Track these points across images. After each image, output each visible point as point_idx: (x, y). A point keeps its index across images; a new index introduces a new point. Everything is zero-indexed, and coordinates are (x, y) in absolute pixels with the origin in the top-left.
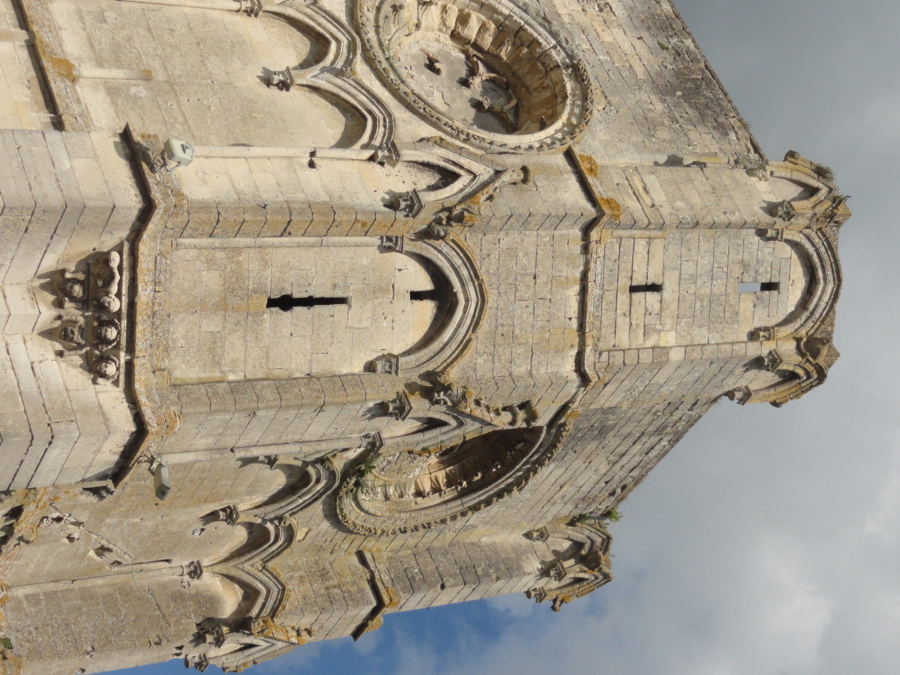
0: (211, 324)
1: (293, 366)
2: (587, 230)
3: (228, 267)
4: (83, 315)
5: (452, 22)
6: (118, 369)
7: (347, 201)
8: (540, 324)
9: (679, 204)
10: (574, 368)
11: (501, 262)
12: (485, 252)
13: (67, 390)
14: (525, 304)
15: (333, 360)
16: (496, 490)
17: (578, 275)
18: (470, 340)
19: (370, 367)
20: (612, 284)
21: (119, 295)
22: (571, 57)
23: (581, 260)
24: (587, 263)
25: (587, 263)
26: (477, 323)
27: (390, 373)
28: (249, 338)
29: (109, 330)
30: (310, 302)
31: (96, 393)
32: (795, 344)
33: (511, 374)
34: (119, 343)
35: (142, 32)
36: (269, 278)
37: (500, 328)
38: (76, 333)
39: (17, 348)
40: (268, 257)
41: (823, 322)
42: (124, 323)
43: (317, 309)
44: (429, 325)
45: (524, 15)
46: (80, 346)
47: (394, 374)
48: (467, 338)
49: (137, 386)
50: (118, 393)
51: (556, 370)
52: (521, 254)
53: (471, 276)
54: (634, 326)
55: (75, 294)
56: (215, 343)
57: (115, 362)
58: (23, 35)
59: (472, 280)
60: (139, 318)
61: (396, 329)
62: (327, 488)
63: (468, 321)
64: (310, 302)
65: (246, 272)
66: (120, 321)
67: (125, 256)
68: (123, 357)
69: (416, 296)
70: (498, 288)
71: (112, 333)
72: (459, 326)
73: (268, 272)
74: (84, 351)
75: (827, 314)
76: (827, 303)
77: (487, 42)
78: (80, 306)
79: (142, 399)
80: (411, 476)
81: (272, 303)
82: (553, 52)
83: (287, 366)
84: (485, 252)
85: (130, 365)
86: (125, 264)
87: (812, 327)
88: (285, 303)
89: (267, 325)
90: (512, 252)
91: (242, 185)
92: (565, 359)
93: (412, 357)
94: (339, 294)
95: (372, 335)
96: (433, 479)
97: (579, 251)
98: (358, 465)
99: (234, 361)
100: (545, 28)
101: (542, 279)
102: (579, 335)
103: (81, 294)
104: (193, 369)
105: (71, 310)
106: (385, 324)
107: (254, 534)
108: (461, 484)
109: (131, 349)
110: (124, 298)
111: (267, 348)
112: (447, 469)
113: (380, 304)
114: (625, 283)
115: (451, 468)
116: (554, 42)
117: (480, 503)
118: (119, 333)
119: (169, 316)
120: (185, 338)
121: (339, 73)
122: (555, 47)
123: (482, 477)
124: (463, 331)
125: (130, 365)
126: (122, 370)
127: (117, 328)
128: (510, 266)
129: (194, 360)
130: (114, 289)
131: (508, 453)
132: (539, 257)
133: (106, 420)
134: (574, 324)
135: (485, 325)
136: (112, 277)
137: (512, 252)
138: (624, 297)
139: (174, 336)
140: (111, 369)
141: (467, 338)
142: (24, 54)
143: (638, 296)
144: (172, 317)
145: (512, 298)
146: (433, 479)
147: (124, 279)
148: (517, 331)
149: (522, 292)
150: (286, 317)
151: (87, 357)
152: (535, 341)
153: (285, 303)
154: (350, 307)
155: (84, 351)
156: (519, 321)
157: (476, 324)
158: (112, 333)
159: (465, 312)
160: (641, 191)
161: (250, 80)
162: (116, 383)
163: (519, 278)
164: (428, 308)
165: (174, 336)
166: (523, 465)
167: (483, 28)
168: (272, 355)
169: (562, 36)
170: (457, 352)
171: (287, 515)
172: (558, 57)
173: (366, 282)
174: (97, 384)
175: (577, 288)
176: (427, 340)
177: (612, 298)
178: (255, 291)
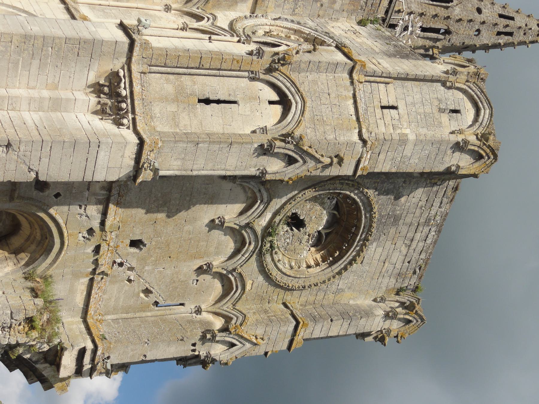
0: (172, 108)
1: (215, 130)
2: (351, 73)
3: (177, 83)
4: (110, 101)
6: (129, 121)
8: (336, 116)
10: (358, 138)
11: (310, 86)
12: (301, 81)
13: (105, 129)
14: (326, 106)
15: (234, 129)
16: (348, 260)
17: (351, 95)
18: (301, 120)
20: (370, 104)
21: (125, 88)
23: (351, 88)
24: (354, 90)
25: (354, 90)
26: (303, 113)
27: (264, 133)
28: (191, 115)
29: (122, 104)
30: (218, 102)
31: (119, 131)
32: (475, 137)
33: (325, 138)
34: (128, 110)
36: (197, 89)
37: (316, 117)
38: (108, 109)
40: (195, 80)
41: (488, 127)
42: (129, 101)
43: (223, 105)
44: (280, 116)
45: (316, 33)
46: (111, 115)
47: (265, 134)
48: (299, 119)
49: (138, 128)
50: (131, 131)
51: (349, 138)
52: (319, 83)
53: (296, 91)
54: (387, 125)
55: (105, 91)
56: (174, 116)
57: (127, 118)
59: (297, 93)
60: (135, 98)
61: (264, 116)
62: (256, 248)
63: (299, 112)
64: (218, 102)
65: (185, 86)
66: (127, 100)
67: (126, 71)
69: (271, 103)
70: (311, 98)
71: (124, 105)
72: (295, 114)
73: (196, 87)
74: (112, 117)
75: (489, 124)
76: (488, 119)
78: (108, 97)
80: (302, 257)
81: (200, 101)
83: (212, 129)
84: (301, 81)
85: (134, 120)
86: (126, 74)
87: (483, 130)
88: (207, 101)
89: (199, 110)
90: (315, 82)
92: (353, 134)
94: (232, 99)
95: (252, 119)
96: (315, 259)
97: (349, 84)
98: (268, 229)
99: (185, 125)
100: (327, 36)
101: (333, 95)
102: (357, 123)
103: (108, 91)
104: (166, 128)
105: (104, 99)
106: (258, 114)
107: (225, 287)
108: (329, 259)
109: (133, 112)
110: (127, 89)
111: (201, 121)
112: (321, 253)
113: (254, 104)
114: (377, 104)
115: (323, 252)
116: (332, 40)
117: (341, 270)
118: (127, 105)
119: (151, 103)
120: (160, 113)
122: (333, 42)
123: (339, 254)
124: (297, 116)
125: (134, 120)
126: (131, 122)
127: (126, 103)
128: (315, 89)
129: (166, 124)
130: (122, 85)
131: (349, 236)
132: (329, 85)
134: (354, 118)
135: (307, 114)
136: (121, 80)
137: (315, 82)
139: (155, 112)
140: (125, 121)
141: (299, 119)
143: (386, 111)
144: (152, 104)
145: (319, 103)
146: (315, 259)
147: (126, 81)
148: (325, 119)
152: (335, 124)
153: (207, 101)
154: (239, 105)
155: (112, 117)
156: (325, 114)
157: (303, 113)
158: (124, 105)
159: (296, 108)
162: (128, 128)
163: (321, 94)
165: (155, 112)
166: (358, 242)
168: (203, 124)
170: (296, 126)
171: (238, 267)
173: (245, 94)
174: (120, 128)
175: (352, 101)
177: (372, 110)
178: (191, 95)
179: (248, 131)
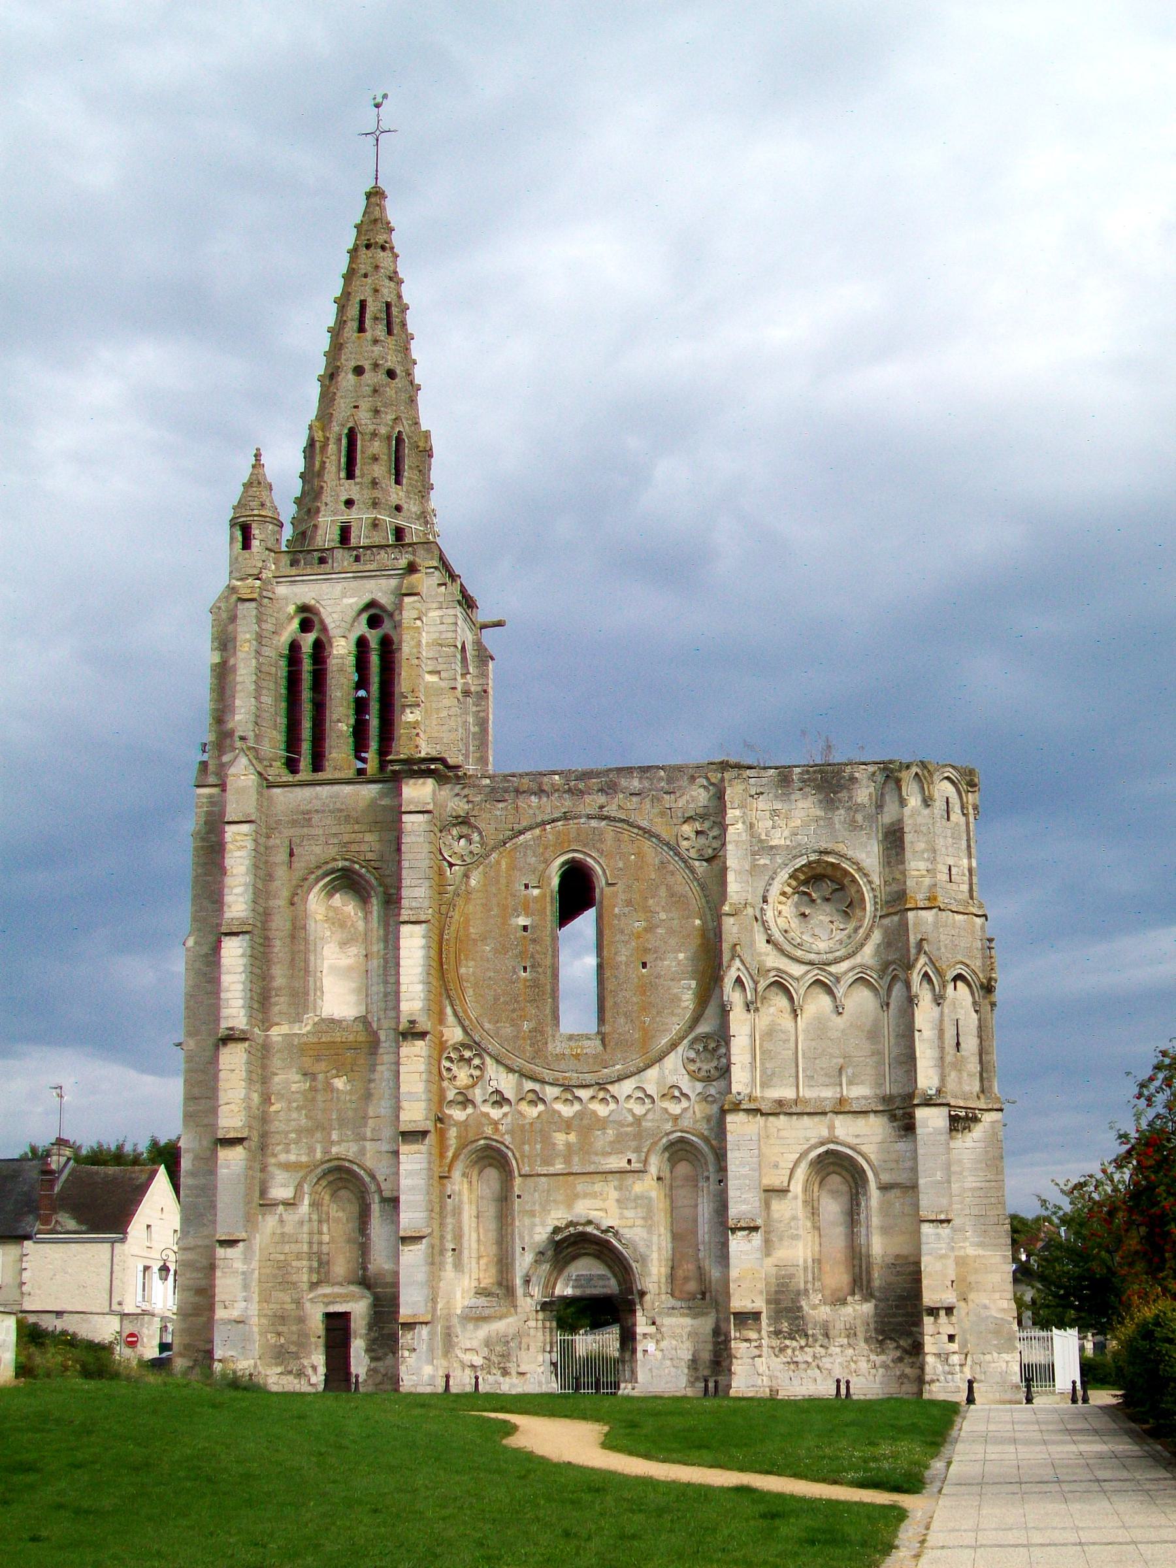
0: (965, 1075)
2: (940, 910)
5: (784, 899)
7: (938, 1022)
9: (926, 855)
19: (976, 1011)
22: (815, 852)
30: (958, 1034)
35: (817, 1061)
39: (967, 1145)
58: (830, 1115)
64: (958, 1034)
68: (977, 1112)
71: (970, 1115)
77: (794, 883)
79: (990, 1106)
82: (811, 859)
85: (980, 1110)
88: (958, 1044)
91: (932, 1063)
93: (976, 995)
109: (974, 1109)
114: (949, 886)
121: (838, 980)
125: (980, 1110)
133: (996, 1121)
135: (968, 962)
138: (954, 886)
142: (841, 1117)
143: (953, 880)
149: (956, 942)
150: (963, 1045)
151: (972, 1122)
153: (958, 1044)
157: (967, 966)
158: (970, 1115)
160: (917, 873)
161: (839, 1021)
164: (960, 984)
167: (789, 885)
169: (804, 851)
172: (813, 857)
176: (969, 985)
179: (975, 1016)
